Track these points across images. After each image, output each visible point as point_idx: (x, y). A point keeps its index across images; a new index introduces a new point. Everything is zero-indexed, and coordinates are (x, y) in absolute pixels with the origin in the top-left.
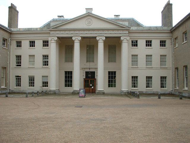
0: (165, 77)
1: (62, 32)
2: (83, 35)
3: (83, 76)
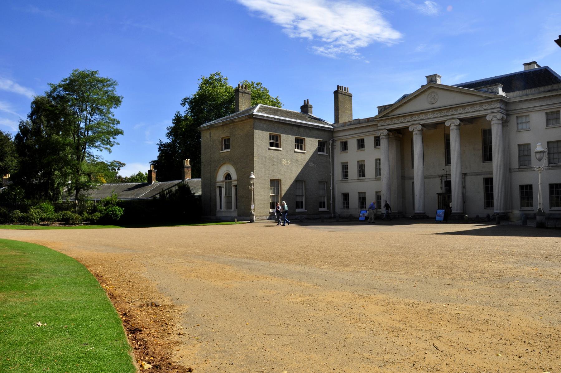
3: (442, 188)
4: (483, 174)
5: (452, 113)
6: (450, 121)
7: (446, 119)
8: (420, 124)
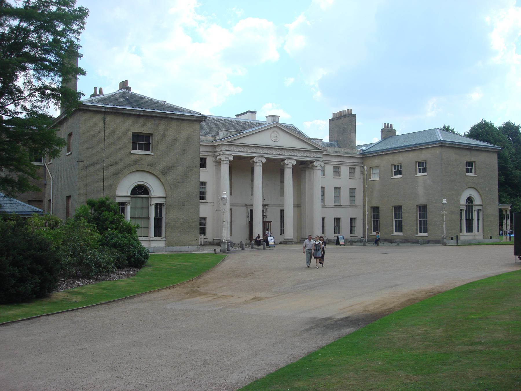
0: (355, 219)
1: (239, 149)
2: (268, 155)
4: (281, 207)
5: (290, 154)
6: (289, 160)
7: (286, 158)
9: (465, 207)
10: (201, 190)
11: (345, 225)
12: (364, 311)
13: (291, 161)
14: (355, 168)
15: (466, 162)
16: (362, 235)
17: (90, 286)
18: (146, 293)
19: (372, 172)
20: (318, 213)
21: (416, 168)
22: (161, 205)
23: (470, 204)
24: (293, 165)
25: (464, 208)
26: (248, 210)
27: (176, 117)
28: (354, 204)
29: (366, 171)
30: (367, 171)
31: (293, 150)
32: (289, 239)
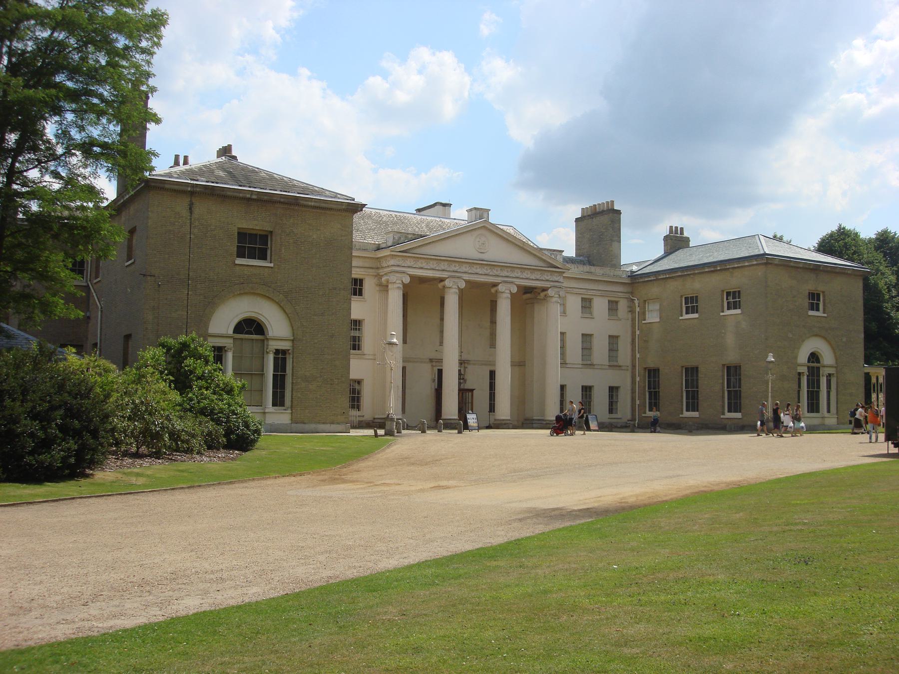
0: (617, 388)
3: (434, 381)
4: (490, 365)
5: (507, 274)
7: (500, 281)
8: (464, 279)
9: (806, 368)
10: (353, 333)
11: (600, 399)
12: (620, 503)
13: (509, 285)
14: (619, 301)
15: (808, 291)
16: (629, 417)
17: (158, 467)
18: (253, 479)
19: (647, 309)
20: (554, 376)
21: (723, 301)
22: (284, 352)
23: (816, 364)
24: (511, 294)
25: (804, 370)
26: (433, 369)
27: (313, 204)
28: (615, 364)
29: (637, 307)
30: (639, 306)
31: (512, 267)
32: (503, 420)
